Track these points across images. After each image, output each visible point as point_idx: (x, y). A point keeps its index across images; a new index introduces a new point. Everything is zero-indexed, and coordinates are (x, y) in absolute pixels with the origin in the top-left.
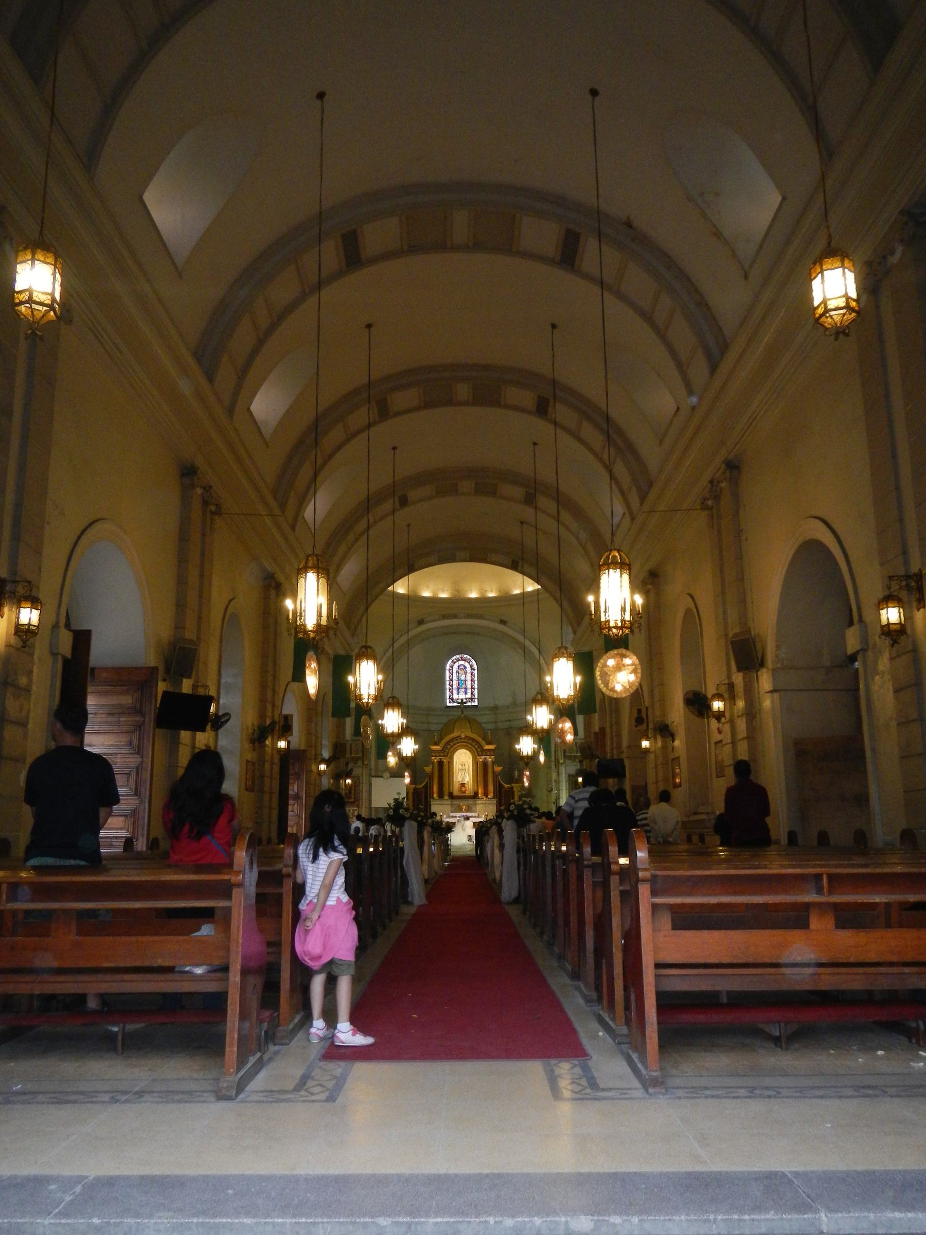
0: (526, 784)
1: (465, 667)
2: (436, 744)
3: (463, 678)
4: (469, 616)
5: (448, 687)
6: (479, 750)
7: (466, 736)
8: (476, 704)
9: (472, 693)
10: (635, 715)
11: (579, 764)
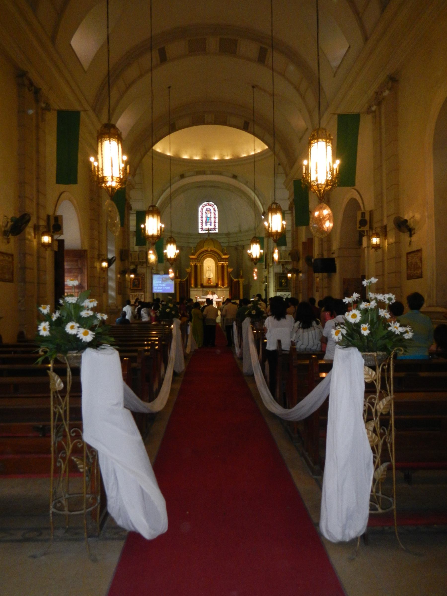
0: (255, 278)
1: (210, 210)
2: (193, 254)
3: (209, 216)
4: (213, 173)
5: (200, 221)
6: (219, 258)
7: (211, 250)
8: (217, 231)
9: (214, 225)
10: (359, 218)
11: (282, 266)
